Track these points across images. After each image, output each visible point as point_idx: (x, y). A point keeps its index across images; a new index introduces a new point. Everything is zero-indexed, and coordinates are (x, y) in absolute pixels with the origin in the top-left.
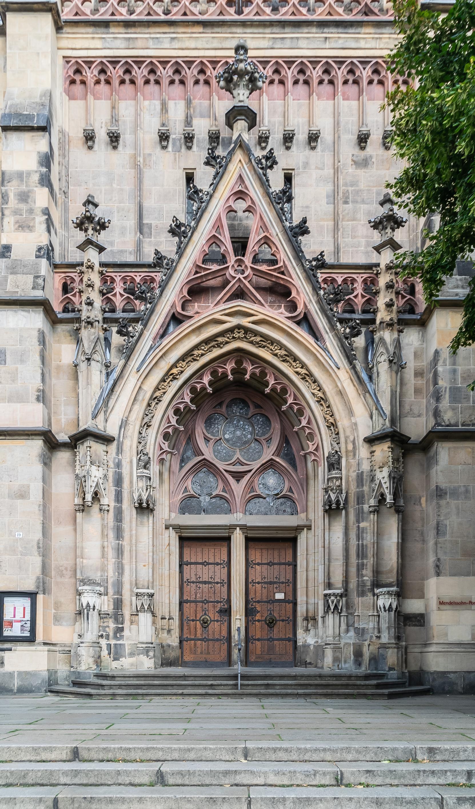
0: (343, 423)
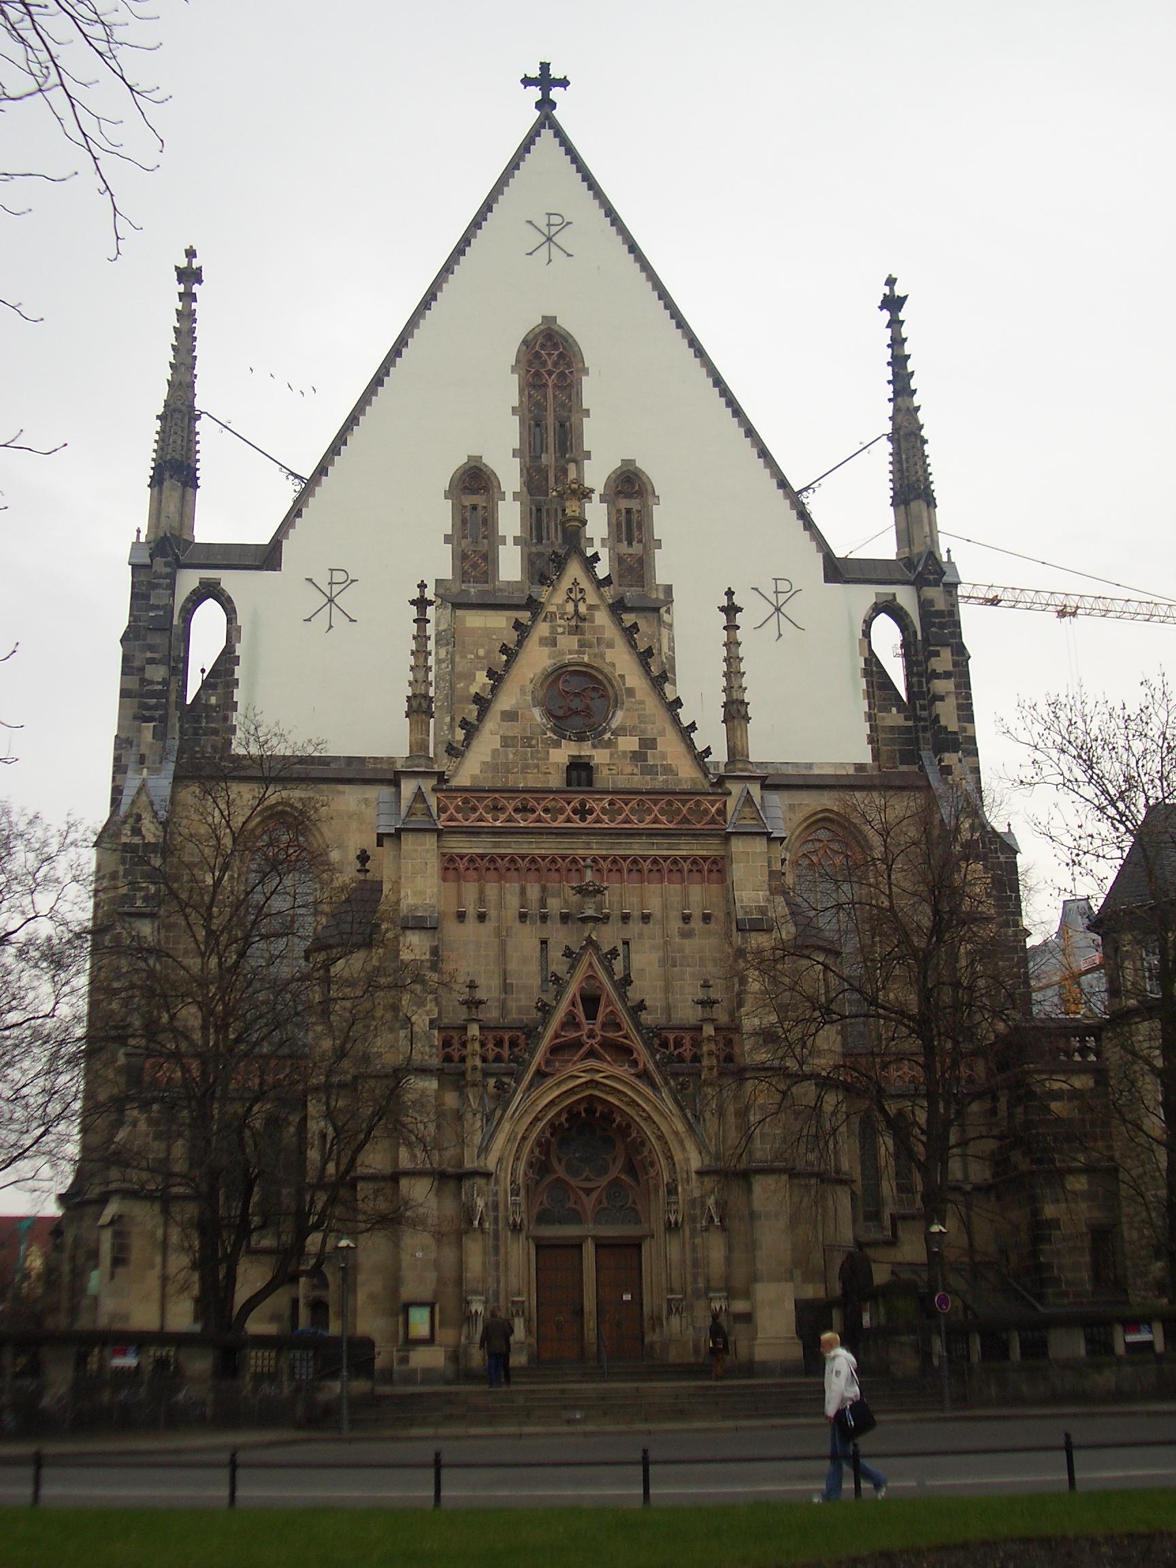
0: (678, 1156)
